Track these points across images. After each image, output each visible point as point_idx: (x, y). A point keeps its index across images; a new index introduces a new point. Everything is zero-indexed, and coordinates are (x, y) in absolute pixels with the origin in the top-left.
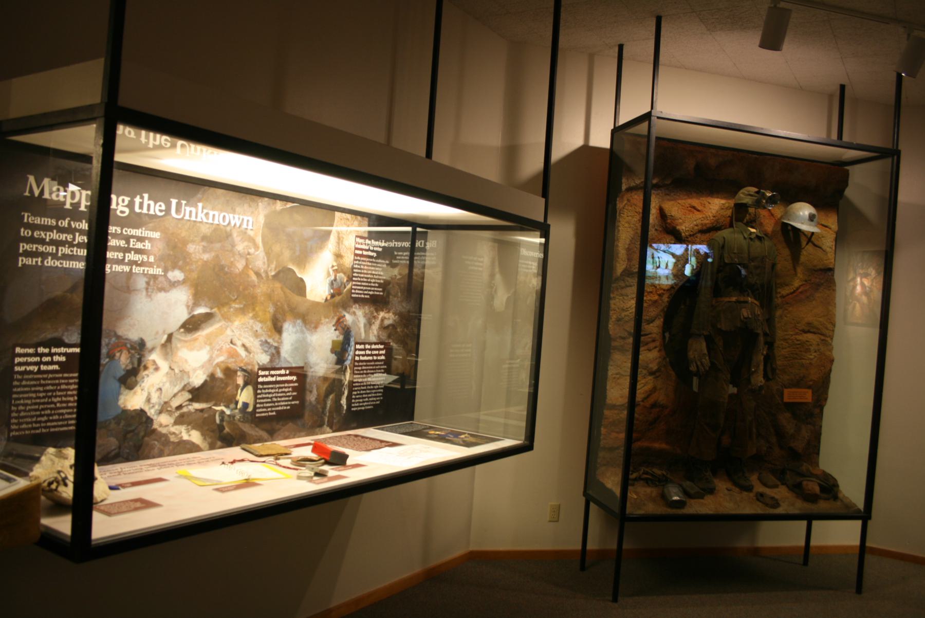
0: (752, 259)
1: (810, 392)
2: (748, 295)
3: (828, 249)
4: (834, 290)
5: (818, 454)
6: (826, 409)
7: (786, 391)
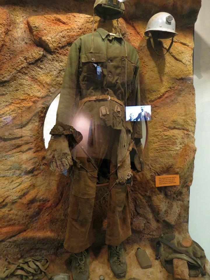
0: (111, 60)
1: (178, 176)
2: (108, 94)
3: (188, 63)
4: (194, 94)
5: (187, 222)
6: (191, 188)
7: (157, 178)
